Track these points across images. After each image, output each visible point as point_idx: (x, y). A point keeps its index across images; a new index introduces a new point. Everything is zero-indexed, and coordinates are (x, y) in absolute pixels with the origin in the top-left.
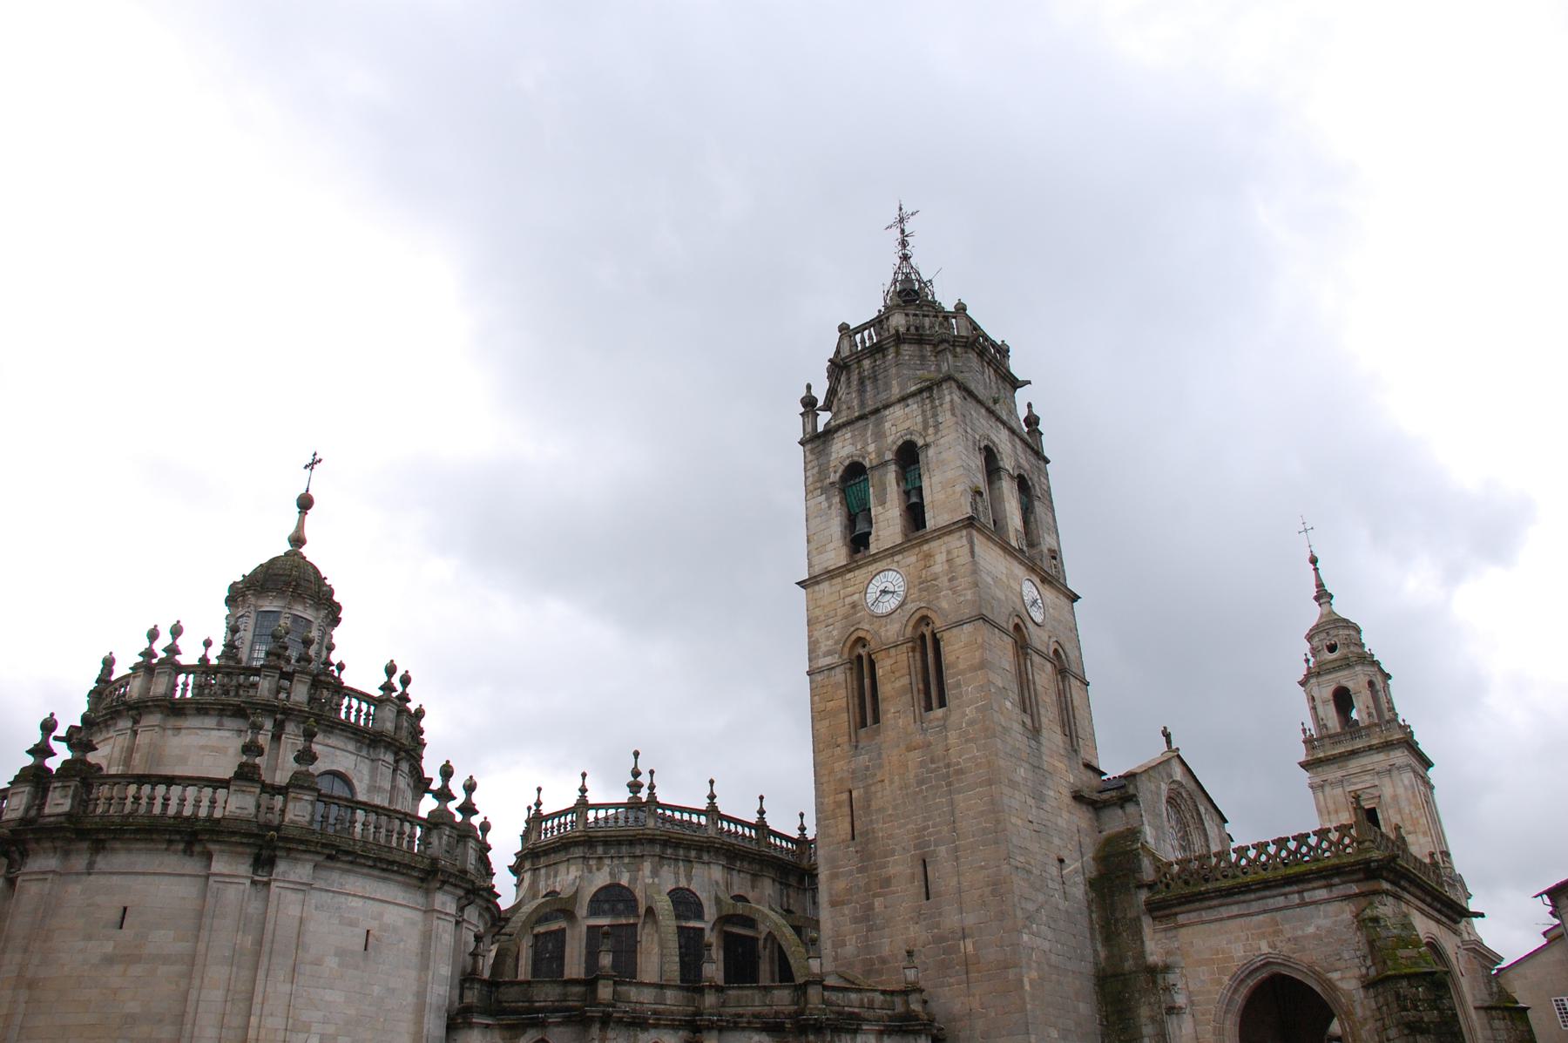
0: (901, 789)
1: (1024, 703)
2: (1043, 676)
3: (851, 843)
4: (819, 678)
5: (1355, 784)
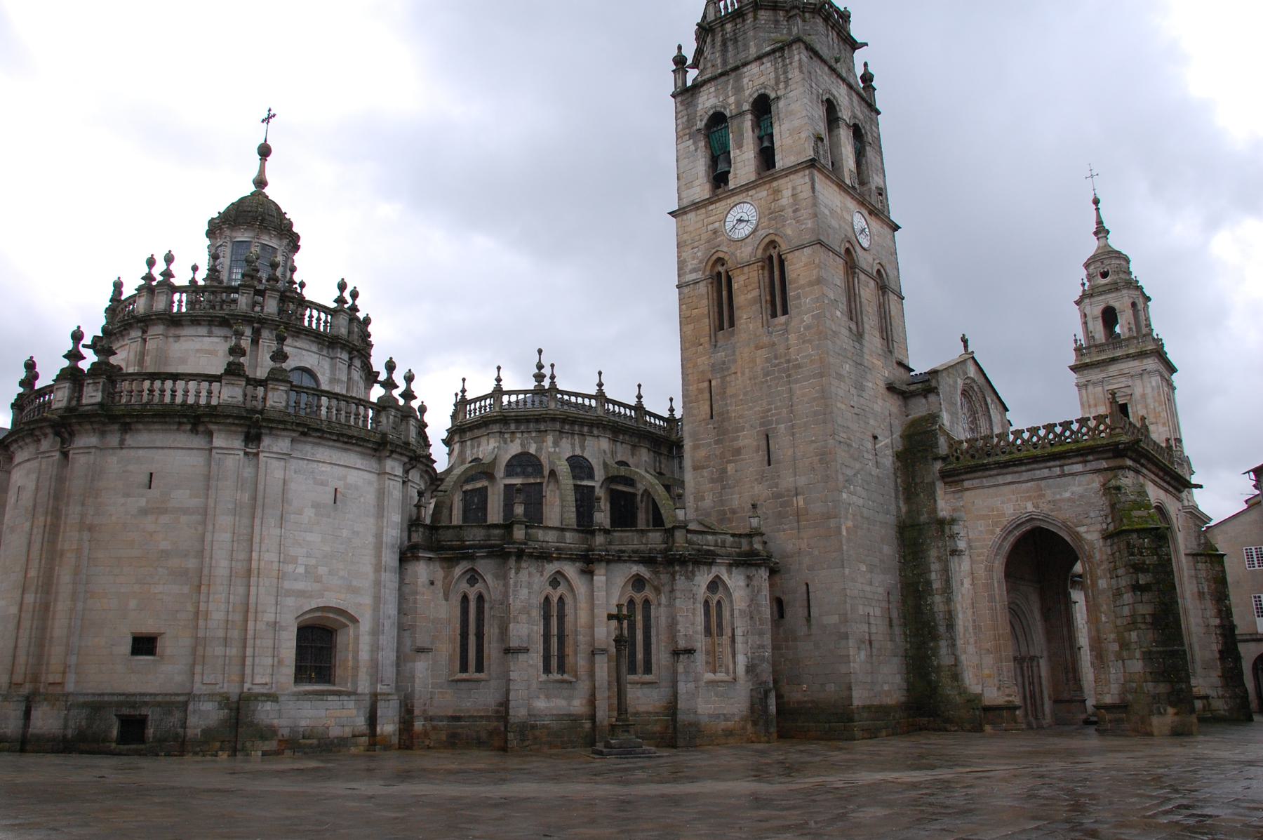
0: (750, 379)
1: (851, 312)
2: (867, 291)
3: (710, 421)
4: (686, 290)
5: (1113, 384)
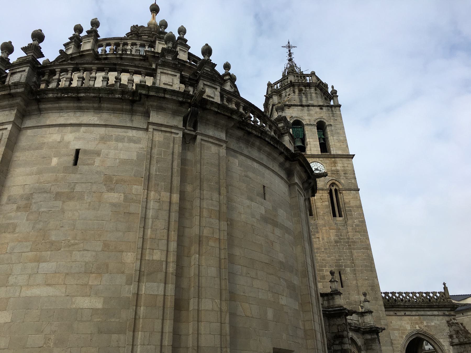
0: (327, 243)
